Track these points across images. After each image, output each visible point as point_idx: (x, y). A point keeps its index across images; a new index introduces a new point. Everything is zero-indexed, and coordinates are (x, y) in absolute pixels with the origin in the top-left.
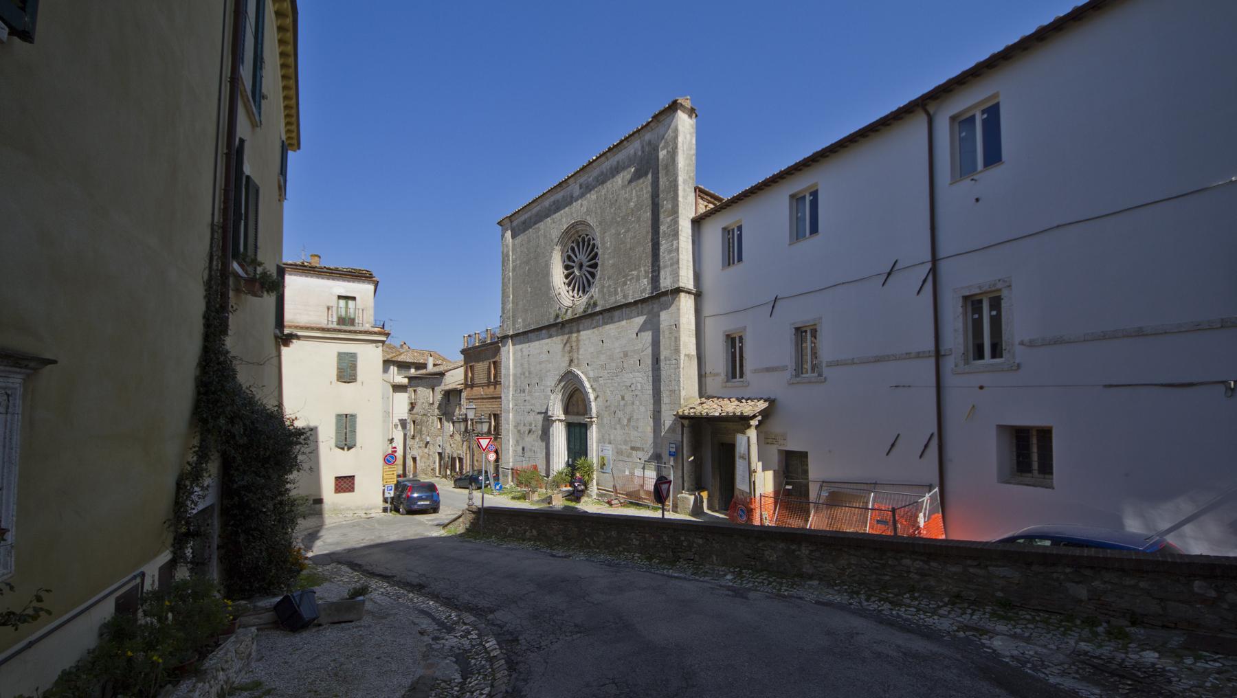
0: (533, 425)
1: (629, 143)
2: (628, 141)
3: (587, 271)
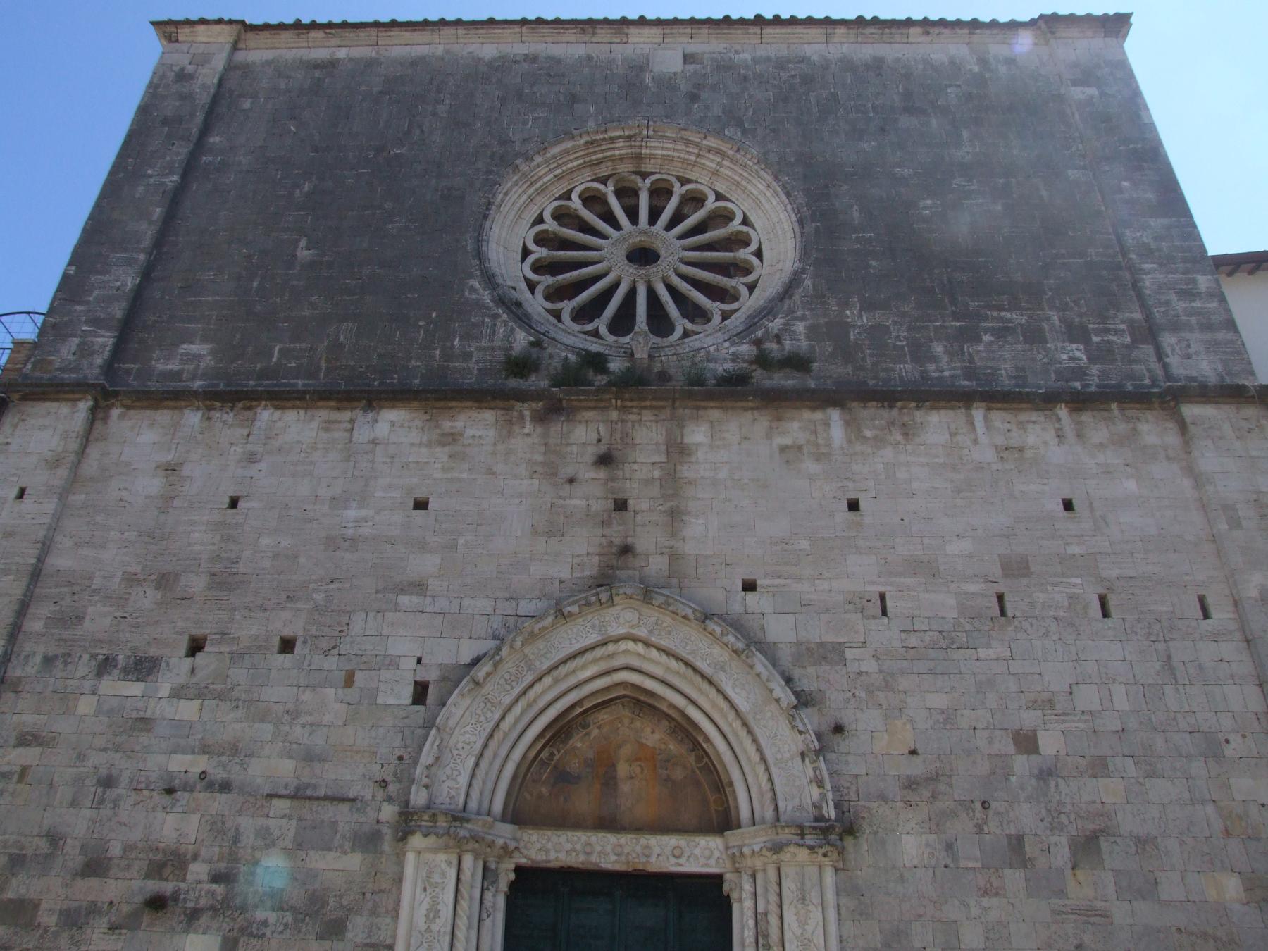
0: (198, 870)
1: (924, 39)
2: (928, 33)
3: (631, 294)
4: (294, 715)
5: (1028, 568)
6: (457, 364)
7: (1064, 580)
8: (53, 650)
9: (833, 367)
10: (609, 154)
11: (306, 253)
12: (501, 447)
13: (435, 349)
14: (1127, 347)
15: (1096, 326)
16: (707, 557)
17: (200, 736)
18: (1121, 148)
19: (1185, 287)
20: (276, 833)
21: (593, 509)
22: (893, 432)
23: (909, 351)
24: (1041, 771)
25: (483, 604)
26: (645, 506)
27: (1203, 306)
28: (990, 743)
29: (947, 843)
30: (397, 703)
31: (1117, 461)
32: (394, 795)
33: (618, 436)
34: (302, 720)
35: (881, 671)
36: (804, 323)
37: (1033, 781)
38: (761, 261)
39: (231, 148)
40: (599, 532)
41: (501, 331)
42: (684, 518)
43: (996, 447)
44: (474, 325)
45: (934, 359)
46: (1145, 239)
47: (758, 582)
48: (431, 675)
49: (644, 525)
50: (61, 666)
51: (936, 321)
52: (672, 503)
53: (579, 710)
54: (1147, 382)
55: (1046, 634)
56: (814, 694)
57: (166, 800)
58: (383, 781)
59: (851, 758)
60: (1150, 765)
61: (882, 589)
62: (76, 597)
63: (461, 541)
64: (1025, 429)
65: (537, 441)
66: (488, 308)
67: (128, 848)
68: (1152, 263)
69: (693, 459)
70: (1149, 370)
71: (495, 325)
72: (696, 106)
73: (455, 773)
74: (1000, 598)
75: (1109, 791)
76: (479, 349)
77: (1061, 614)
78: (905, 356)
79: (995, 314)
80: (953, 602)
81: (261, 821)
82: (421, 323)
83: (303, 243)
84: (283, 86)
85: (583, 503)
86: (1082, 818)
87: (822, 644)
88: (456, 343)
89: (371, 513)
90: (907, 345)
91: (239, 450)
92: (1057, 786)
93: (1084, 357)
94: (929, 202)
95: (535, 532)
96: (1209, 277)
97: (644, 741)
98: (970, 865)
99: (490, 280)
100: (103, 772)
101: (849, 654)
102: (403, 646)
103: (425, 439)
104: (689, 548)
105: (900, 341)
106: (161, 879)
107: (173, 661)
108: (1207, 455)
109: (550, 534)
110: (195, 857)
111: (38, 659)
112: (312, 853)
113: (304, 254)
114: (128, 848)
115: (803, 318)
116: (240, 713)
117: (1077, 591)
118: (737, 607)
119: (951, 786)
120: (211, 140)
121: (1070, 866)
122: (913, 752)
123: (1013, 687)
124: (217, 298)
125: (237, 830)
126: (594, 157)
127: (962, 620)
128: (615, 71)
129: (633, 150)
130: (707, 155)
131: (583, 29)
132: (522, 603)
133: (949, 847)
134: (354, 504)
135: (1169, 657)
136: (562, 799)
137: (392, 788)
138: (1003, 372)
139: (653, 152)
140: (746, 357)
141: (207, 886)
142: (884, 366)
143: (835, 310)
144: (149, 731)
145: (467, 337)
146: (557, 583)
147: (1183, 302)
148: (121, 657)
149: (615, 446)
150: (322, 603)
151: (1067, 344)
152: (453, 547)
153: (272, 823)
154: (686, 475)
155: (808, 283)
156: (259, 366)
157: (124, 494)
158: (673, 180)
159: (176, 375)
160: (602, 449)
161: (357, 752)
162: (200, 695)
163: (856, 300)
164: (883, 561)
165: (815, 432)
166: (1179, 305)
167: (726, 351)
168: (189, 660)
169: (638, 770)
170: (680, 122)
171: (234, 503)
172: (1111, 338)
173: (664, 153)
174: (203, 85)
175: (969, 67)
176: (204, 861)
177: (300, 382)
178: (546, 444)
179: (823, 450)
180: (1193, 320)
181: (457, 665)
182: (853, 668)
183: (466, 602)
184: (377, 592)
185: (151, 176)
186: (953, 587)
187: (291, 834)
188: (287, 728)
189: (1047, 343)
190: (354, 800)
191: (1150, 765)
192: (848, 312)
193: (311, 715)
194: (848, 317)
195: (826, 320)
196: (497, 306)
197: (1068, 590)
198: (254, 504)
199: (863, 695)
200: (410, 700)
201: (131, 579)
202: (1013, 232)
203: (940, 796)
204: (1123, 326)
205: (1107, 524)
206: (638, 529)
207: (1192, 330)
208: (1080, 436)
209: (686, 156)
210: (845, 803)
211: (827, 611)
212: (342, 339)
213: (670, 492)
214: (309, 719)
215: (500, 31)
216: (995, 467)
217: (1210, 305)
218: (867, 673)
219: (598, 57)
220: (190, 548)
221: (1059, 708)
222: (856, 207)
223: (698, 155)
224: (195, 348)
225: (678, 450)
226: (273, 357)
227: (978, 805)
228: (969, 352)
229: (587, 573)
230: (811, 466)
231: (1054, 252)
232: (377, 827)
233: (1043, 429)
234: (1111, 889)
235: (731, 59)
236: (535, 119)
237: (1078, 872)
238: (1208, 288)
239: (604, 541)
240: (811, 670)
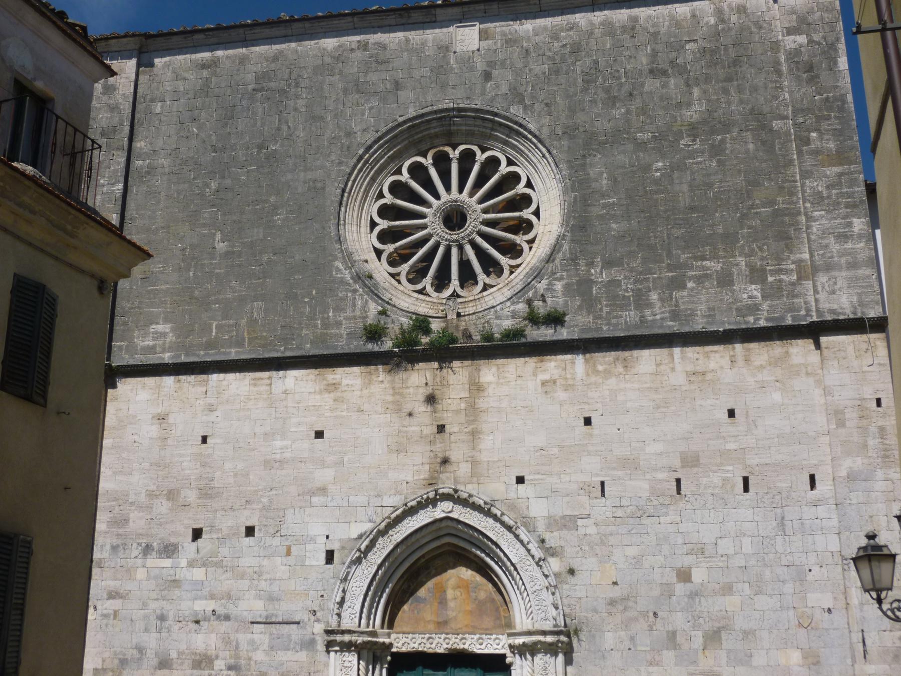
4: (260, 574)
5: (698, 460)
6: (333, 331)
7: (721, 468)
8: (116, 542)
9: (580, 317)
10: (425, 133)
11: (221, 244)
12: (365, 392)
13: (317, 320)
14: (793, 284)
15: (772, 268)
16: (494, 462)
17: (208, 589)
18: (816, 98)
19: (843, 230)
20: (258, 642)
21: (425, 432)
22: (618, 365)
23: (634, 301)
24: (691, 592)
25: (362, 499)
26: (456, 429)
27: (853, 246)
28: (662, 576)
29: (631, 637)
30: (317, 563)
31: (770, 379)
32: (321, 618)
33: (438, 380)
34: (265, 576)
35: (598, 533)
36: (562, 283)
37: (686, 599)
38: (539, 219)
39: (154, 151)
40: (428, 448)
41: (359, 303)
42: (481, 436)
43: (687, 372)
44: (342, 299)
45: (650, 305)
46: (820, 189)
47: (525, 478)
48: (334, 546)
49: (456, 442)
50: (122, 551)
51: (655, 274)
52: (472, 426)
53: (423, 560)
54: (803, 312)
55: (704, 505)
56: (557, 549)
57: (194, 626)
58: (314, 611)
59: (577, 588)
60: (759, 587)
61: (602, 479)
62: (121, 508)
63: (346, 459)
64: (708, 357)
65: (387, 386)
66: (349, 285)
67: (180, 654)
68: (822, 210)
69: (486, 394)
70: (806, 303)
71: (355, 298)
72: (489, 84)
73: (353, 605)
74: (678, 481)
75: (731, 602)
76: (346, 318)
77: (716, 491)
78: (630, 305)
79: (699, 263)
80: (647, 486)
81: (250, 636)
82: (306, 300)
83: (218, 236)
84: (182, 89)
85: (417, 429)
86: (713, 620)
87: (564, 517)
88: (331, 314)
89: (290, 442)
90: (633, 296)
91: (202, 403)
92: (700, 601)
93: (760, 296)
94: (660, 164)
95: (390, 451)
96: (863, 220)
97: (462, 576)
98: (643, 649)
99: (349, 259)
100: (159, 612)
101: (580, 522)
102: (317, 529)
103: (317, 388)
104: (484, 457)
105: (628, 292)
106: (201, 669)
107: (186, 545)
108: (832, 372)
109: (399, 451)
110: (217, 657)
111: (108, 547)
112: (279, 652)
113: (221, 246)
114: (180, 654)
115: (561, 279)
116: (229, 574)
117: (728, 475)
118: (512, 495)
119: (636, 603)
120: (138, 145)
121: (701, 648)
122: (615, 583)
123: (680, 541)
124: (168, 286)
125: (237, 641)
126: (416, 137)
127: (652, 498)
128: (427, 53)
129: (444, 128)
130: (498, 128)
131: (400, 15)
132: (385, 498)
133: (632, 639)
134: (279, 437)
135: (783, 518)
136: (416, 612)
137: (318, 614)
138: (699, 312)
139: (459, 128)
140: (521, 314)
141: (226, 672)
142: (615, 314)
143: (583, 271)
144: (179, 587)
145: (338, 309)
146: (405, 483)
147: (838, 244)
148: (155, 544)
149: (437, 387)
150: (267, 504)
151: (748, 285)
152: (340, 463)
153: (256, 637)
154: (482, 406)
155: (566, 247)
156: (204, 339)
157: (136, 438)
158: (475, 148)
159: (151, 349)
160: (429, 390)
161: (298, 594)
162: (204, 565)
163: (599, 260)
164: (604, 460)
165: (565, 369)
166: (835, 247)
167: (507, 309)
168: (194, 544)
169: (459, 594)
170: (477, 102)
171: (204, 440)
172: (782, 277)
173: (468, 128)
174: (124, 94)
175: (707, 19)
176: (223, 659)
177: (233, 350)
178: (393, 388)
179: (570, 382)
180: (843, 261)
181: (350, 539)
182: (581, 531)
183: (352, 499)
184: (299, 495)
185: (103, 186)
186: (648, 476)
187: (267, 641)
188: (256, 582)
189: (734, 285)
190: (298, 623)
191: (759, 587)
192: (593, 271)
193: (269, 573)
194: (592, 275)
195: (577, 279)
196: (355, 282)
197: (723, 475)
198: (218, 441)
199: (587, 548)
200: (325, 562)
201: (151, 495)
202: (722, 187)
203: (629, 609)
204: (793, 266)
205: (756, 426)
206: (453, 445)
207: (840, 269)
208: (747, 360)
209: (484, 130)
210: (573, 614)
211: (568, 495)
212: (255, 315)
213: (472, 418)
214: (269, 576)
215: (337, 22)
216: (684, 388)
217: (858, 246)
218: (590, 535)
219: (414, 39)
220: (183, 472)
221: (707, 553)
222: (605, 175)
223: (492, 129)
224: (160, 328)
225: (476, 388)
226: (212, 332)
227: (651, 614)
228: (676, 297)
229: (422, 477)
230: (561, 395)
231: (750, 203)
232: (312, 636)
233: (721, 357)
234: (724, 661)
236: (371, 108)
237: (706, 652)
238: (860, 230)
239: (432, 454)
240: (556, 534)
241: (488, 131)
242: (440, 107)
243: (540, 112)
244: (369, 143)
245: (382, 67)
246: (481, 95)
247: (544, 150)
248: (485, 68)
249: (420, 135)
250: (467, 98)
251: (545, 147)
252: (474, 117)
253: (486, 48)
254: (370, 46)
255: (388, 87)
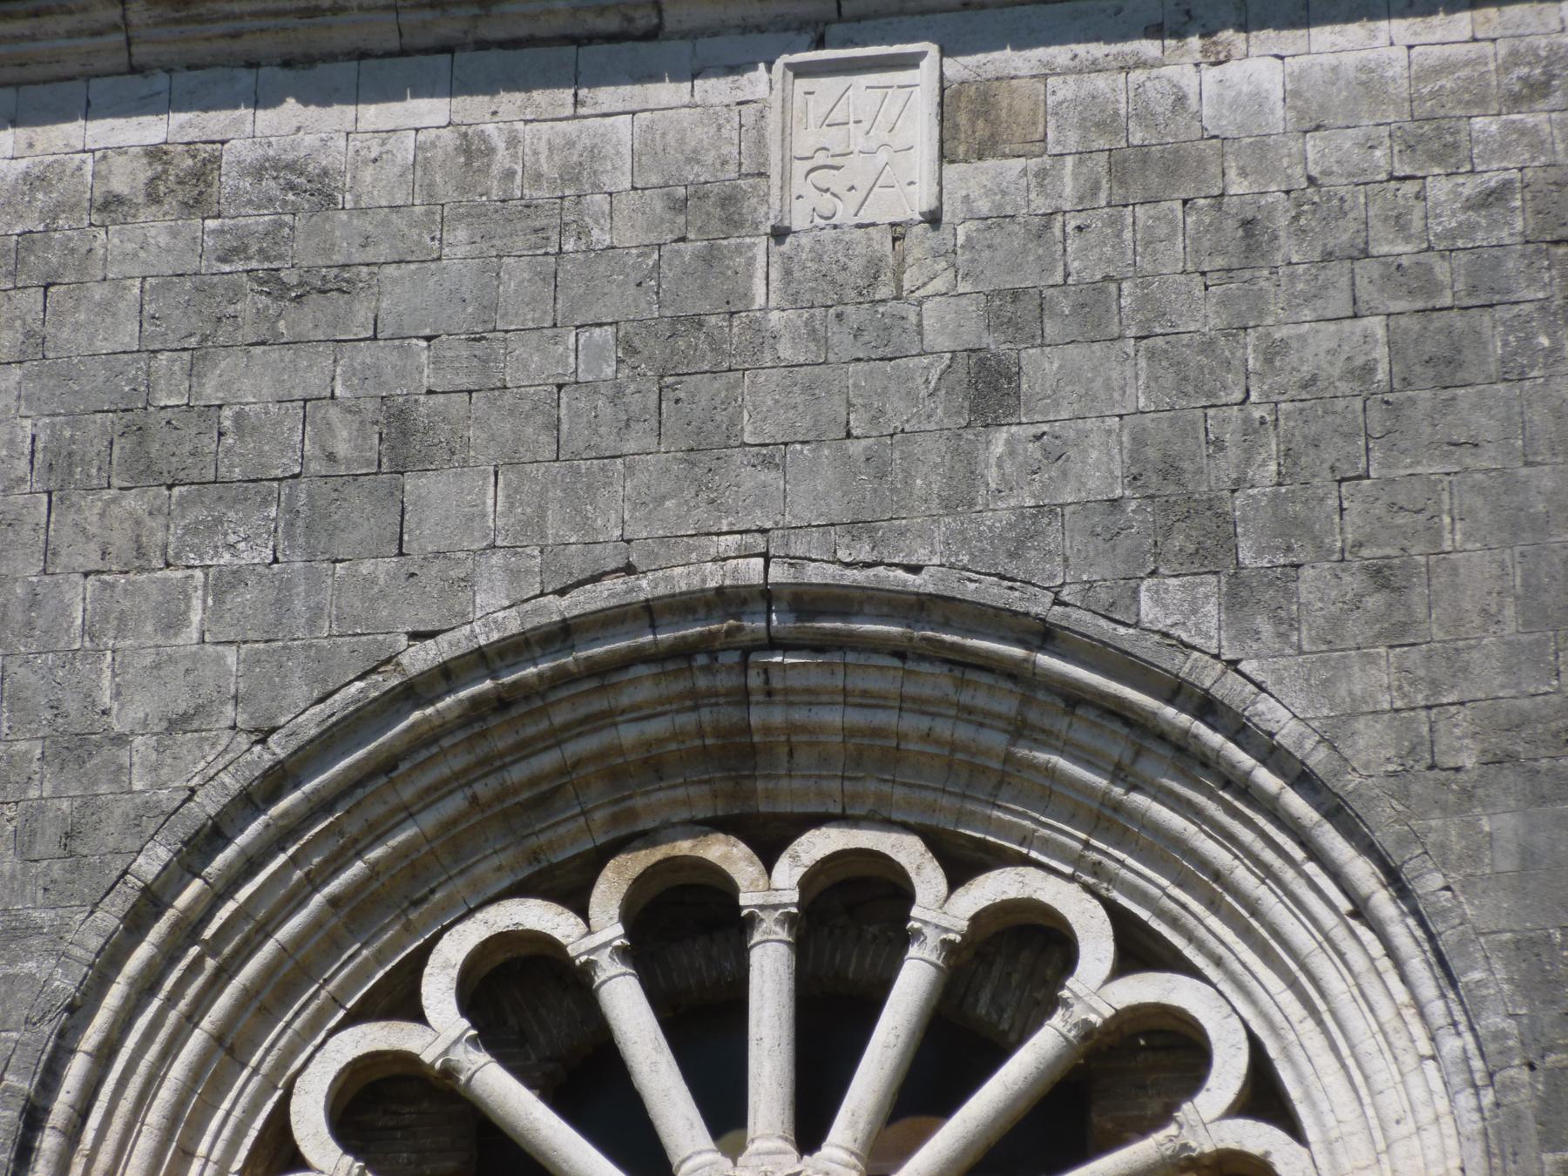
72: (999, 441)
126: (517, 774)
128: (599, 236)
129: (706, 715)
130: (1061, 724)
139: (798, 715)
158: (907, 851)
170: (920, 555)
173: (857, 718)
209: (964, 733)
219: (513, 141)
223: (1020, 730)
235: (1181, 100)
236: (223, 584)
241: (995, 740)
242: (682, 579)
243: (1335, 623)
244: (208, 805)
245: (306, 320)
246: (949, 507)
247: (1362, 871)
248: (973, 333)
249: (547, 761)
250: (858, 526)
251: (1368, 848)
252: (900, 652)
253: (984, 206)
254: (229, 180)
255: (342, 449)
